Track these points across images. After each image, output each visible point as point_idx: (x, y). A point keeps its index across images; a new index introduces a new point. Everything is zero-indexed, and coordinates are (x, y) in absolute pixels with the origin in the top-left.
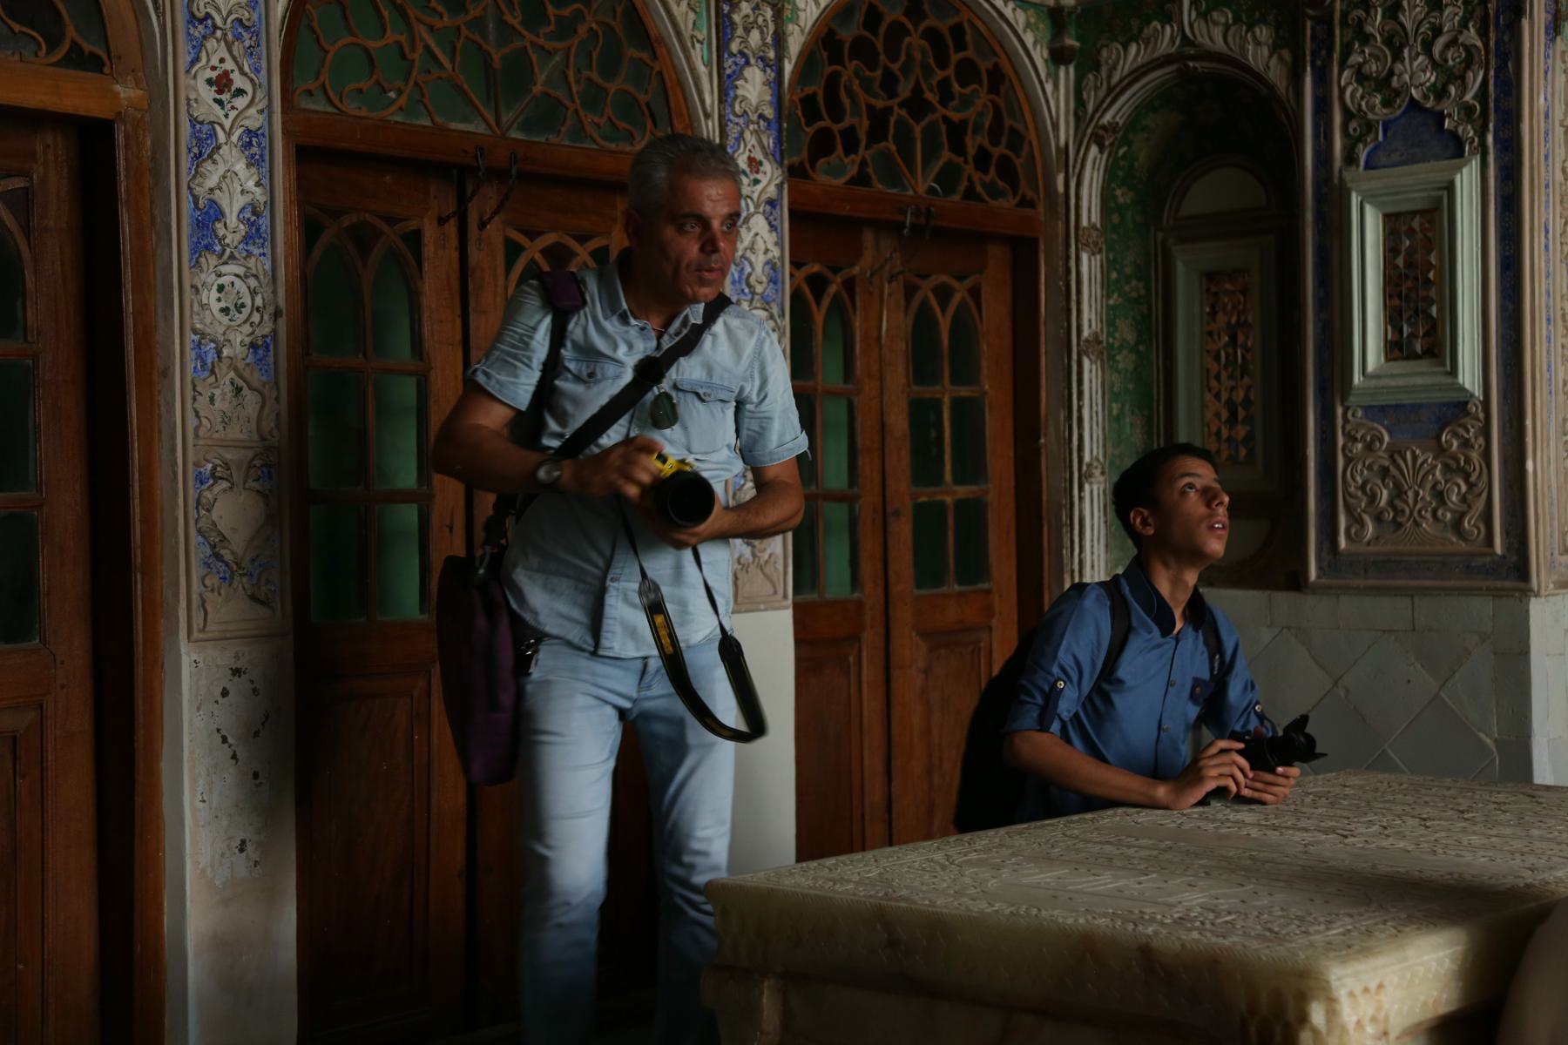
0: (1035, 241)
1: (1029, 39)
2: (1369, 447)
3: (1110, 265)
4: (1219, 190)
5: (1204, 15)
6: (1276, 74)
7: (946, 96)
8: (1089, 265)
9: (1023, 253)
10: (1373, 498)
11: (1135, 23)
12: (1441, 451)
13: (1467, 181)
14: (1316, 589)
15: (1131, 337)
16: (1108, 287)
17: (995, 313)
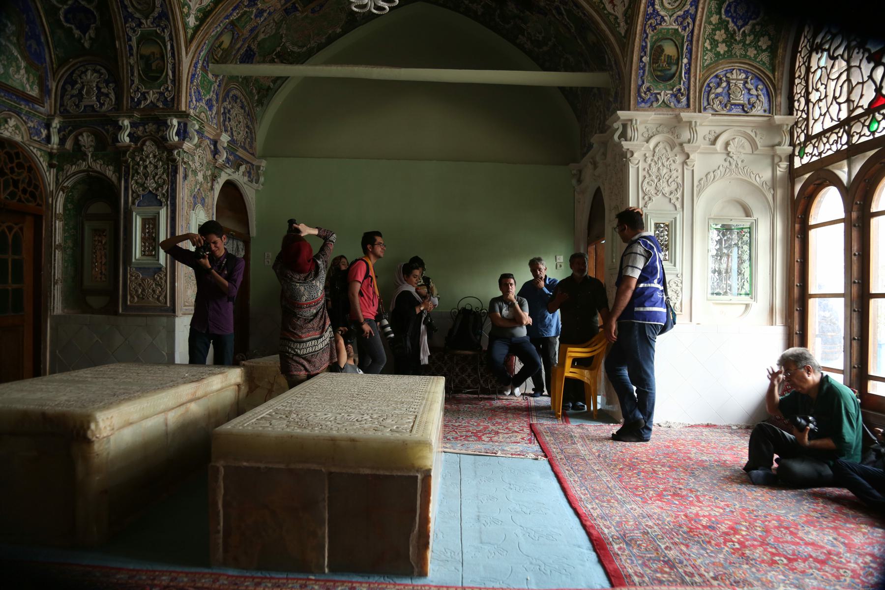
0: (42, 216)
1: (41, 160)
2: (136, 278)
3: (65, 225)
4: (99, 207)
5: (95, 161)
6: (114, 179)
7: (12, 170)
8: (59, 225)
9: (38, 219)
10: (137, 291)
11: (75, 160)
12: (155, 280)
13: (163, 213)
14: (121, 315)
15: (71, 245)
16: (64, 231)
17: (28, 235)
